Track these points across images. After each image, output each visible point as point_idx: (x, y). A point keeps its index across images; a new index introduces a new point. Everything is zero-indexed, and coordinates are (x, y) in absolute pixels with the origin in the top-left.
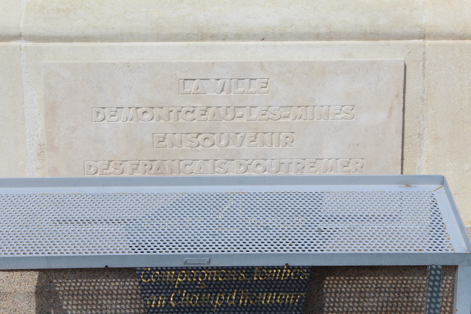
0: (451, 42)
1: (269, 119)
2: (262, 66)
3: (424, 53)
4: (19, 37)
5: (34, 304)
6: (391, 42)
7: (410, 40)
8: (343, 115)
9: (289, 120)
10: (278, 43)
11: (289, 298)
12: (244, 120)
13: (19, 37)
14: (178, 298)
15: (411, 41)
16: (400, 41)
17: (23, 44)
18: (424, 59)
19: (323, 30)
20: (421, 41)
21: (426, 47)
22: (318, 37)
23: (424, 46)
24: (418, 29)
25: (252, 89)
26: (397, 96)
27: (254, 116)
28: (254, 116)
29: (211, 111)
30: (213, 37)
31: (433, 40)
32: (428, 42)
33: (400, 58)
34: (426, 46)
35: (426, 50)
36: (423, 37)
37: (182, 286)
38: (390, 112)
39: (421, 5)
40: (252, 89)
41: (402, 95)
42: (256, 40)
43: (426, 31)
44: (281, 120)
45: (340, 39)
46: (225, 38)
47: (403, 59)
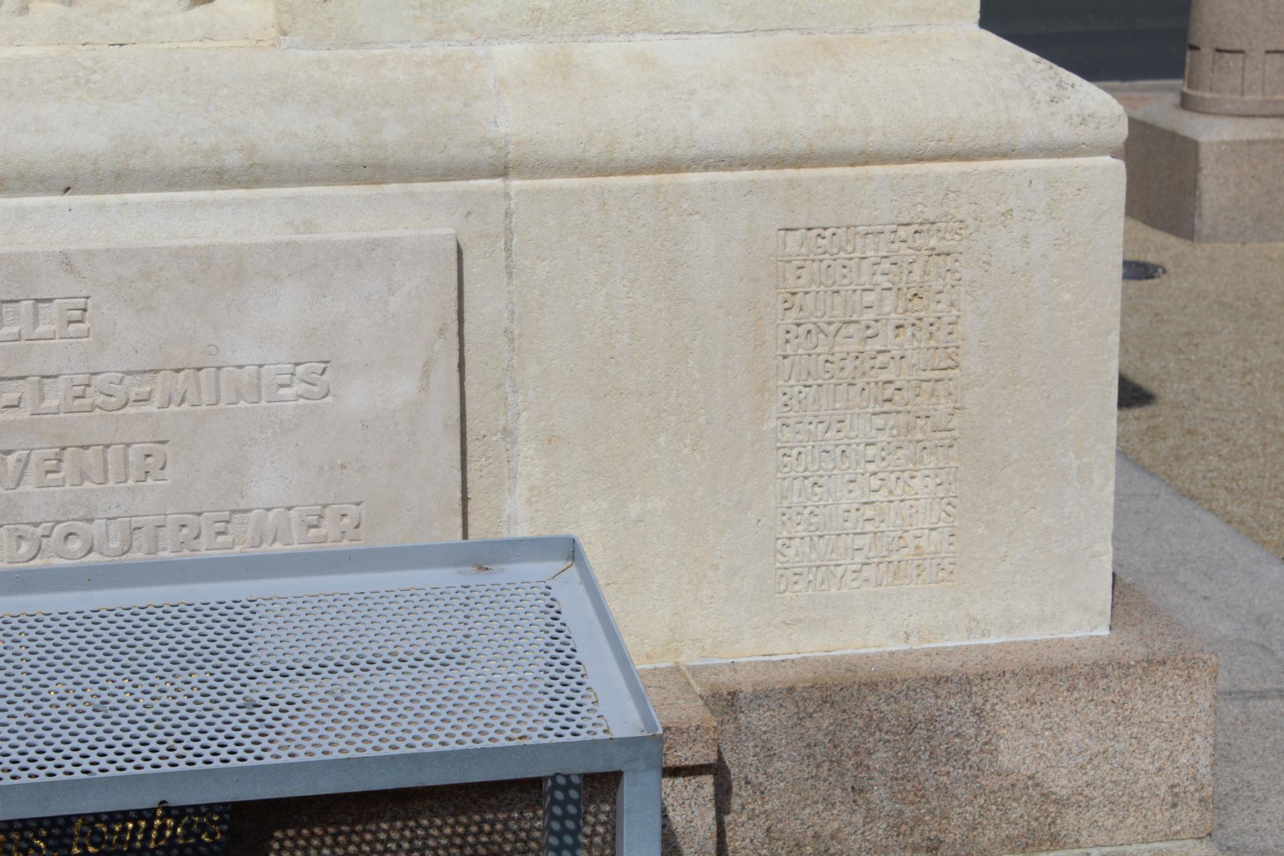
0: (576, 182)
1: (94, 407)
2: (67, 262)
3: (508, 214)
6: (419, 187)
7: (469, 179)
8: (299, 388)
9: (152, 408)
12: (23, 414)
15: (471, 182)
16: (443, 183)
18: (509, 231)
19: (233, 160)
20: (498, 182)
21: (510, 198)
22: (220, 178)
23: (507, 195)
24: (489, 151)
25: (42, 329)
26: (442, 332)
27: (51, 403)
28: (51, 403)
31: (528, 179)
32: (516, 184)
33: (443, 230)
34: (512, 194)
35: (512, 206)
36: (503, 171)
38: (427, 372)
39: (492, 86)
40: (42, 329)
41: (454, 327)
42: (48, 191)
43: (510, 157)
44: (130, 410)
47: (453, 231)
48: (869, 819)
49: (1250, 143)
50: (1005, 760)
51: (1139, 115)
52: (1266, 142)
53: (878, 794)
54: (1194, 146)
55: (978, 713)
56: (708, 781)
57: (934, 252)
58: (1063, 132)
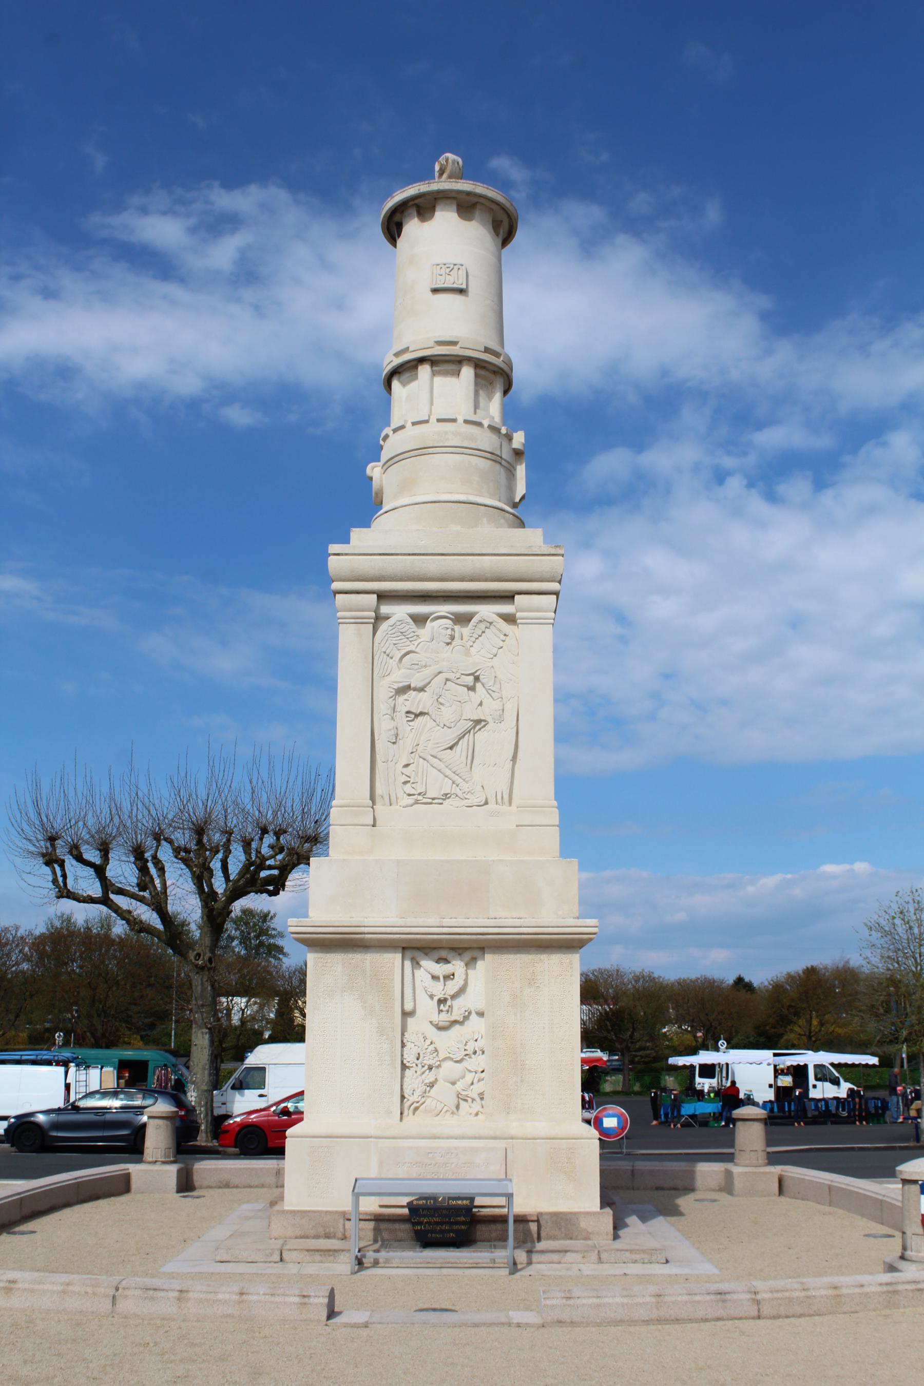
0: (522, 1141)
4: (371, 1137)
5: (372, 1234)
10: (461, 1140)
11: (463, 1227)
13: (371, 1137)
14: (425, 1227)
17: (372, 1140)
19: (477, 1136)
22: (475, 1138)
27: (453, 1167)
29: (437, 1165)
30: (439, 1138)
32: (514, 1140)
36: (512, 1138)
37: (426, 1223)
45: (483, 1139)
46: (443, 1138)
48: (562, 1233)
49: (746, 1172)
50: (581, 1226)
51: (726, 1167)
52: (750, 1172)
53: (563, 1230)
54: (732, 1172)
55: (577, 1218)
56: (536, 1223)
57: (572, 1152)
58: (590, 1136)
